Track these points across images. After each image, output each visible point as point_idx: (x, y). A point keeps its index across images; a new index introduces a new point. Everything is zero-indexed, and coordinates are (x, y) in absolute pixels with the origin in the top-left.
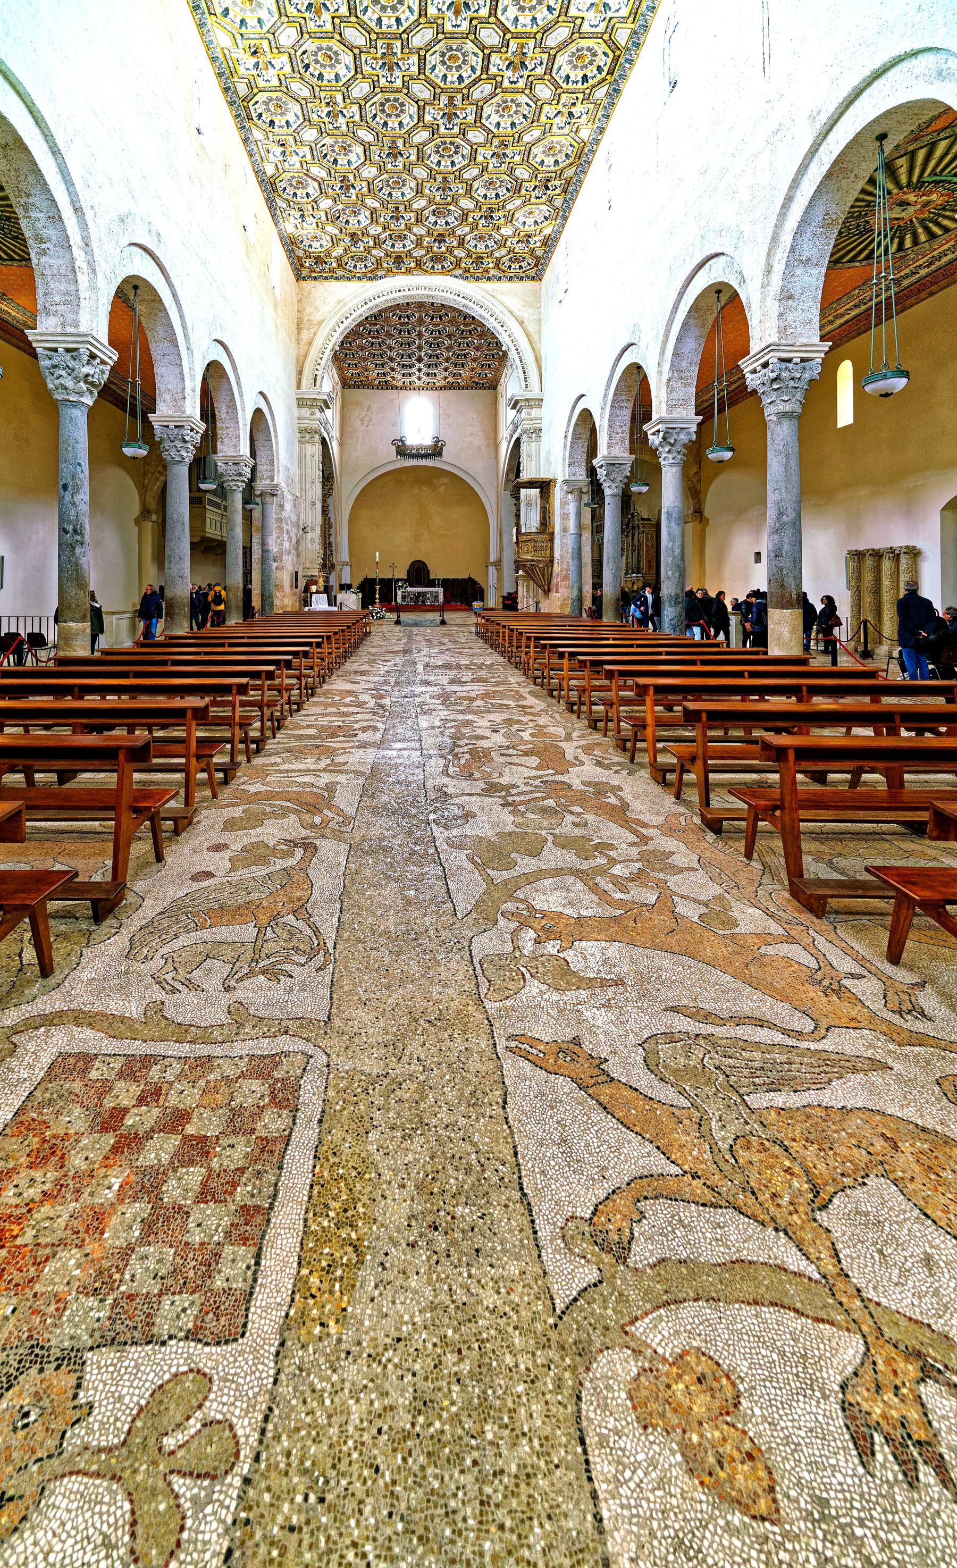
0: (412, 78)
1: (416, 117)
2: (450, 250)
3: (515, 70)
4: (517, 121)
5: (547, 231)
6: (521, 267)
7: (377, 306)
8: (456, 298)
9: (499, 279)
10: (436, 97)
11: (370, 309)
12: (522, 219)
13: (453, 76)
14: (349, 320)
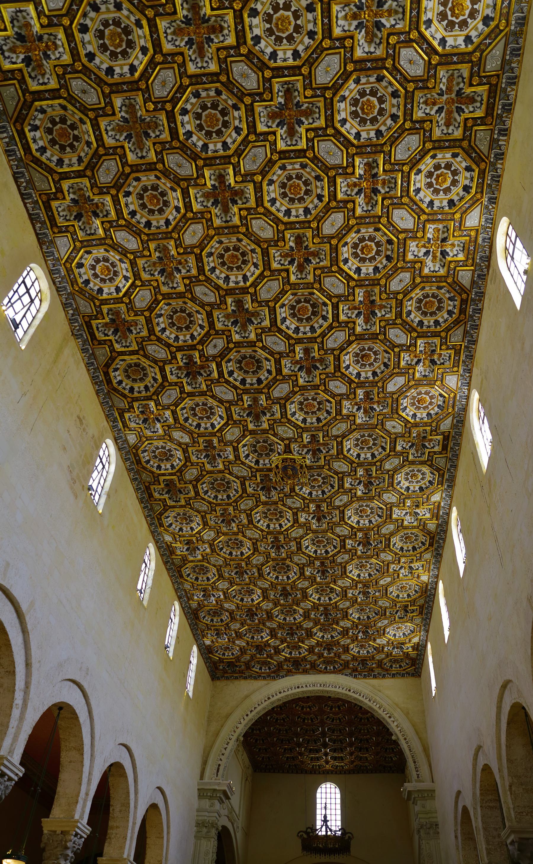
0: (292, 553)
5: (416, 640)
6: (400, 666)
7: (279, 700)
9: (384, 677)
11: (272, 703)
12: (392, 632)
14: (253, 713)
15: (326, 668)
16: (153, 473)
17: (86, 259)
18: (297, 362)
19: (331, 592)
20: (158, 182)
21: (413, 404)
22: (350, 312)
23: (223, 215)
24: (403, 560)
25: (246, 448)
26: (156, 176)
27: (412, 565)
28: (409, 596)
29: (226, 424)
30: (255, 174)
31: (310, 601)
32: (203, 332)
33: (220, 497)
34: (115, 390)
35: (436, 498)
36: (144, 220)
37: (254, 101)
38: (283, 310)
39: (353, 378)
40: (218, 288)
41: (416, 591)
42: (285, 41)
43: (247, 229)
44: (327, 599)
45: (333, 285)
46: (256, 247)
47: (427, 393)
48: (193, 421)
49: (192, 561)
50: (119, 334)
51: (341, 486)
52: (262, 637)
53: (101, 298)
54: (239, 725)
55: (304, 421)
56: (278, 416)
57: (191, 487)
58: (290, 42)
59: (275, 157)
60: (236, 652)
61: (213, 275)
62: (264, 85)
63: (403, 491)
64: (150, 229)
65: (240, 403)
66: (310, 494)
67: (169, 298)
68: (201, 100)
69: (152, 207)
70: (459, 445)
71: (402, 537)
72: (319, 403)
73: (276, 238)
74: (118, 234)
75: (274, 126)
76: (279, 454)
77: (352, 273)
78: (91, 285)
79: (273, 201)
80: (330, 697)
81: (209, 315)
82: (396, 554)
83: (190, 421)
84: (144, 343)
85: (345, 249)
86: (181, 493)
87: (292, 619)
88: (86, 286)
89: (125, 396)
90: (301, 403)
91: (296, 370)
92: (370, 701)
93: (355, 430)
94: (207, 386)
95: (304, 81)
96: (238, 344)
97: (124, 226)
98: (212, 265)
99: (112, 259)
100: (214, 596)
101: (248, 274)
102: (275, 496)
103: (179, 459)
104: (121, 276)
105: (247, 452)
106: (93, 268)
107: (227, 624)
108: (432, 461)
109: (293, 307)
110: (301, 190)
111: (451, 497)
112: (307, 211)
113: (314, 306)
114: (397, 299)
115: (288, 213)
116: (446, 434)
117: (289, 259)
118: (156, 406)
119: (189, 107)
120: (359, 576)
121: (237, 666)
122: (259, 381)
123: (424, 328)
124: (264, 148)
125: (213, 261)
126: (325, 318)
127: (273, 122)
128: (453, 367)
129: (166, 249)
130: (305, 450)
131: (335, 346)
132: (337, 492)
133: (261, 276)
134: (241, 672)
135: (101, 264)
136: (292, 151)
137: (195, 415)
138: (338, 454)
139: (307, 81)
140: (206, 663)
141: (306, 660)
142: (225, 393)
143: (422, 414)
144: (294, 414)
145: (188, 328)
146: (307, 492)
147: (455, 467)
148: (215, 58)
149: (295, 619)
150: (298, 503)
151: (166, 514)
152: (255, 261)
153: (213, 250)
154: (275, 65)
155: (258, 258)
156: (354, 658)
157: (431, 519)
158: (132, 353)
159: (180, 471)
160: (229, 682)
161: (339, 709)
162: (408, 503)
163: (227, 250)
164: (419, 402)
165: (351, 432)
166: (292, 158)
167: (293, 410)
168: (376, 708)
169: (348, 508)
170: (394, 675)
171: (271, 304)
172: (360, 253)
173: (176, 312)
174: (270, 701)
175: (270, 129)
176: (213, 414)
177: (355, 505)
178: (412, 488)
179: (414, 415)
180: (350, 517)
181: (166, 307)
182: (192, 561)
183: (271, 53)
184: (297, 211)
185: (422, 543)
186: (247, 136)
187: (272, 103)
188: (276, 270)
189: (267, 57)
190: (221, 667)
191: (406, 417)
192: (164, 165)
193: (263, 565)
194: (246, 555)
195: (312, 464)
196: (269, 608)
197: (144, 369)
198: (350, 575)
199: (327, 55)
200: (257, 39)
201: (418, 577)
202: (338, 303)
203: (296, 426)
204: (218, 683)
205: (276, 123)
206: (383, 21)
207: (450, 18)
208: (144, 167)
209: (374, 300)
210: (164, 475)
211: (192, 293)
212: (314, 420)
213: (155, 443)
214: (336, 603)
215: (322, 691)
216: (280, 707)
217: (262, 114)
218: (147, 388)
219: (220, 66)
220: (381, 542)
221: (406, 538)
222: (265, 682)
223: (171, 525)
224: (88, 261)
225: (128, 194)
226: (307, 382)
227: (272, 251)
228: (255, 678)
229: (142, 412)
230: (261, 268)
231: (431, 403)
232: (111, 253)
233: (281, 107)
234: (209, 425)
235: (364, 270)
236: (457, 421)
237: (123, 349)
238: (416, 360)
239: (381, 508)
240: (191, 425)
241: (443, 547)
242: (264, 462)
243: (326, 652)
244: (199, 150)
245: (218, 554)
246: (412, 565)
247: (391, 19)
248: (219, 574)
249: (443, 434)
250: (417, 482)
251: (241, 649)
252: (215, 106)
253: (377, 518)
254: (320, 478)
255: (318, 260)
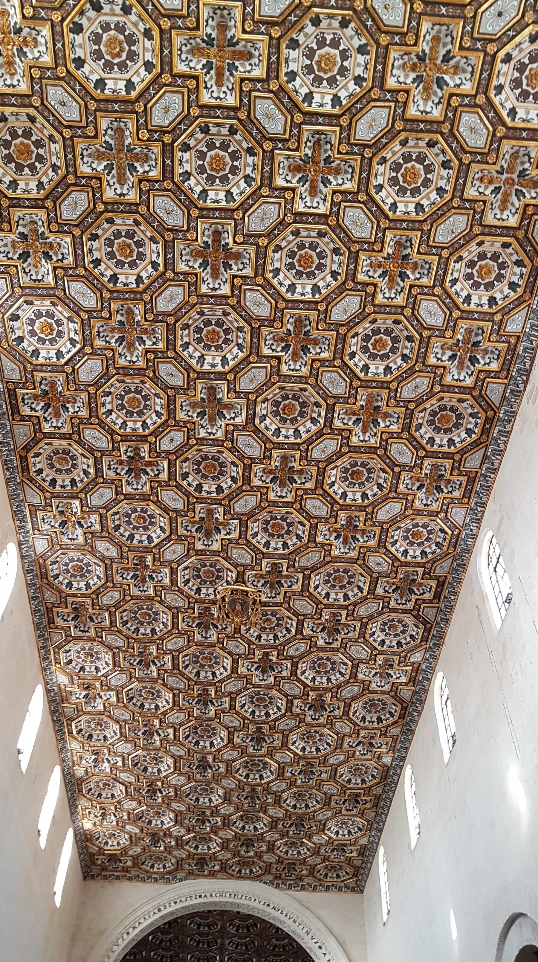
0: (223, 712)
1: (226, 739)
2: (259, 855)
3: (315, 711)
4: (321, 747)
5: (363, 841)
6: (338, 876)
7: (172, 913)
8: (265, 908)
9: (315, 889)
10: (245, 726)
12: (334, 829)
13: (260, 713)
15: (240, 871)
16: (60, 591)
17: (24, 310)
18: (271, 472)
19: (264, 768)
20: (135, 228)
21: (406, 538)
22: (346, 417)
23: (210, 281)
24: (363, 733)
25: (187, 572)
26: (135, 221)
27: (372, 741)
28: (363, 781)
29: (168, 539)
30: (260, 236)
31: (234, 778)
32: (159, 421)
33: (142, 630)
34: (31, 480)
35: (417, 657)
36: (109, 273)
37: (276, 148)
38: (264, 405)
39: (337, 498)
40: (189, 368)
41: (373, 776)
42: (325, 83)
43: (239, 302)
44: (257, 776)
45: (332, 382)
46: (246, 324)
47: (425, 526)
48: (126, 530)
49: (89, 713)
50: (50, 410)
51: (299, 631)
52: (162, 822)
53: (35, 362)
54: (115, 948)
55: (267, 545)
56: (234, 535)
57: (107, 615)
58: (331, 86)
59: (289, 219)
60: (124, 840)
61: (185, 353)
62: (291, 131)
63: (376, 645)
64: (115, 285)
65: (191, 514)
66: (259, 637)
67: (125, 374)
68: (208, 137)
69: (122, 259)
70: (456, 594)
71: (366, 703)
72: (290, 525)
73: (272, 318)
74: (73, 285)
75: (294, 181)
76: (228, 583)
77: (357, 371)
78: (25, 344)
79: (276, 272)
80: (238, 913)
81: (171, 401)
82: (355, 724)
83: (122, 530)
84: (81, 426)
85: (354, 341)
86: (92, 620)
87: (207, 800)
88: (18, 345)
89: (42, 489)
90: (267, 522)
91: (268, 481)
92: (295, 922)
93: (329, 562)
94: (152, 488)
95: (341, 134)
96: (201, 441)
97: (83, 276)
98: (186, 339)
99: (58, 315)
100: (109, 762)
101: (229, 357)
102: (213, 635)
103: (98, 577)
104: (66, 337)
105: (187, 577)
106: (31, 322)
107: (119, 802)
108: (419, 611)
109: (277, 404)
110: (312, 262)
111: (435, 658)
112: (316, 289)
113: (303, 405)
114: (407, 409)
115: (292, 288)
116: (441, 579)
117: (283, 345)
118: (82, 507)
119: (192, 143)
120: (303, 749)
121: (120, 861)
122: (220, 489)
123: (435, 447)
124: (277, 206)
125: (189, 335)
126: (314, 421)
127: (294, 176)
128: (463, 497)
129: (130, 312)
130: (262, 581)
131: (323, 457)
132: (294, 638)
133: (246, 361)
134: (126, 870)
135: (42, 320)
136: (311, 214)
137: (129, 523)
138: (302, 590)
139: (344, 134)
140: (80, 855)
141: (215, 859)
142: (174, 500)
143: (415, 552)
144: (256, 535)
145: (140, 413)
146: (256, 634)
147: (447, 621)
148: (238, 89)
149: (210, 800)
150: (242, 648)
151: (67, 648)
152: (240, 341)
153: (191, 322)
154: (308, 109)
155: (244, 338)
156: (280, 861)
157: (406, 684)
158: (63, 436)
159: (97, 592)
160: (106, 883)
161: (248, 930)
162: (380, 660)
163: (208, 323)
164: (413, 536)
165: (324, 564)
166: (310, 223)
167: (256, 530)
168: (302, 933)
169: (304, 660)
170: (328, 887)
171: (252, 397)
172: (371, 347)
173: (130, 392)
174: (161, 914)
175: (289, 185)
176: (152, 524)
177: (313, 657)
178: (388, 642)
179: (406, 552)
180: (304, 672)
181: (118, 385)
182: (89, 713)
183: (306, 94)
184: (303, 288)
185: (390, 713)
186: (259, 188)
187: (297, 153)
188: (265, 357)
189: (301, 99)
190: (99, 862)
191: (395, 553)
192: (148, 210)
193: (181, 725)
194: (162, 710)
195: (267, 600)
196: (179, 783)
197: (73, 458)
198: (293, 748)
199: (374, 107)
200: (292, 75)
201: (379, 757)
202: (334, 404)
203: (256, 550)
204: (92, 884)
205: (297, 178)
206: (447, 78)
207: (525, 87)
208: (122, 207)
209: (379, 407)
210: (74, 595)
211: (154, 372)
212: (280, 545)
213: (71, 554)
214: (268, 783)
215: (232, 904)
216: (169, 923)
217: (281, 165)
218: (73, 482)
219: (241, 101)
220: (339, 708)
221: (371, 706)
222: (156, 886)
223: (70, 662)
224: (27, 313)
225: (94, 237)
226: (279, 497)
227: (265, 331)
228: (143, 880)
229: (61, 513)
230: (246, 351)
231: (428, 539)
232: (59, 308)
233: (306, 160)
234: (144, 537)
235: (372, 369)
236: (458, 565)
237: (52, 430)
238: (418, 484)
239: (345, 664)
240: (122, 535)
241: (417, 722)
242: (207, 592)
243: (244, 848)
244: (196, 196)
245: (125, 706)
246: (373, 742)
247: (457, 77)
248: (121, 733)
249: (438, 578)
250: (395, 636)
251: (131, 837)
252: (224, 147)
253: (338, 675)
254: (274, 619)
255: (319, 351)
